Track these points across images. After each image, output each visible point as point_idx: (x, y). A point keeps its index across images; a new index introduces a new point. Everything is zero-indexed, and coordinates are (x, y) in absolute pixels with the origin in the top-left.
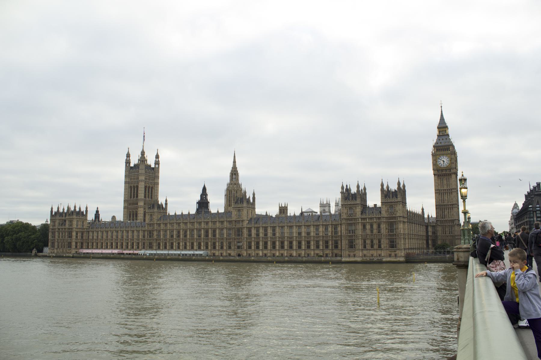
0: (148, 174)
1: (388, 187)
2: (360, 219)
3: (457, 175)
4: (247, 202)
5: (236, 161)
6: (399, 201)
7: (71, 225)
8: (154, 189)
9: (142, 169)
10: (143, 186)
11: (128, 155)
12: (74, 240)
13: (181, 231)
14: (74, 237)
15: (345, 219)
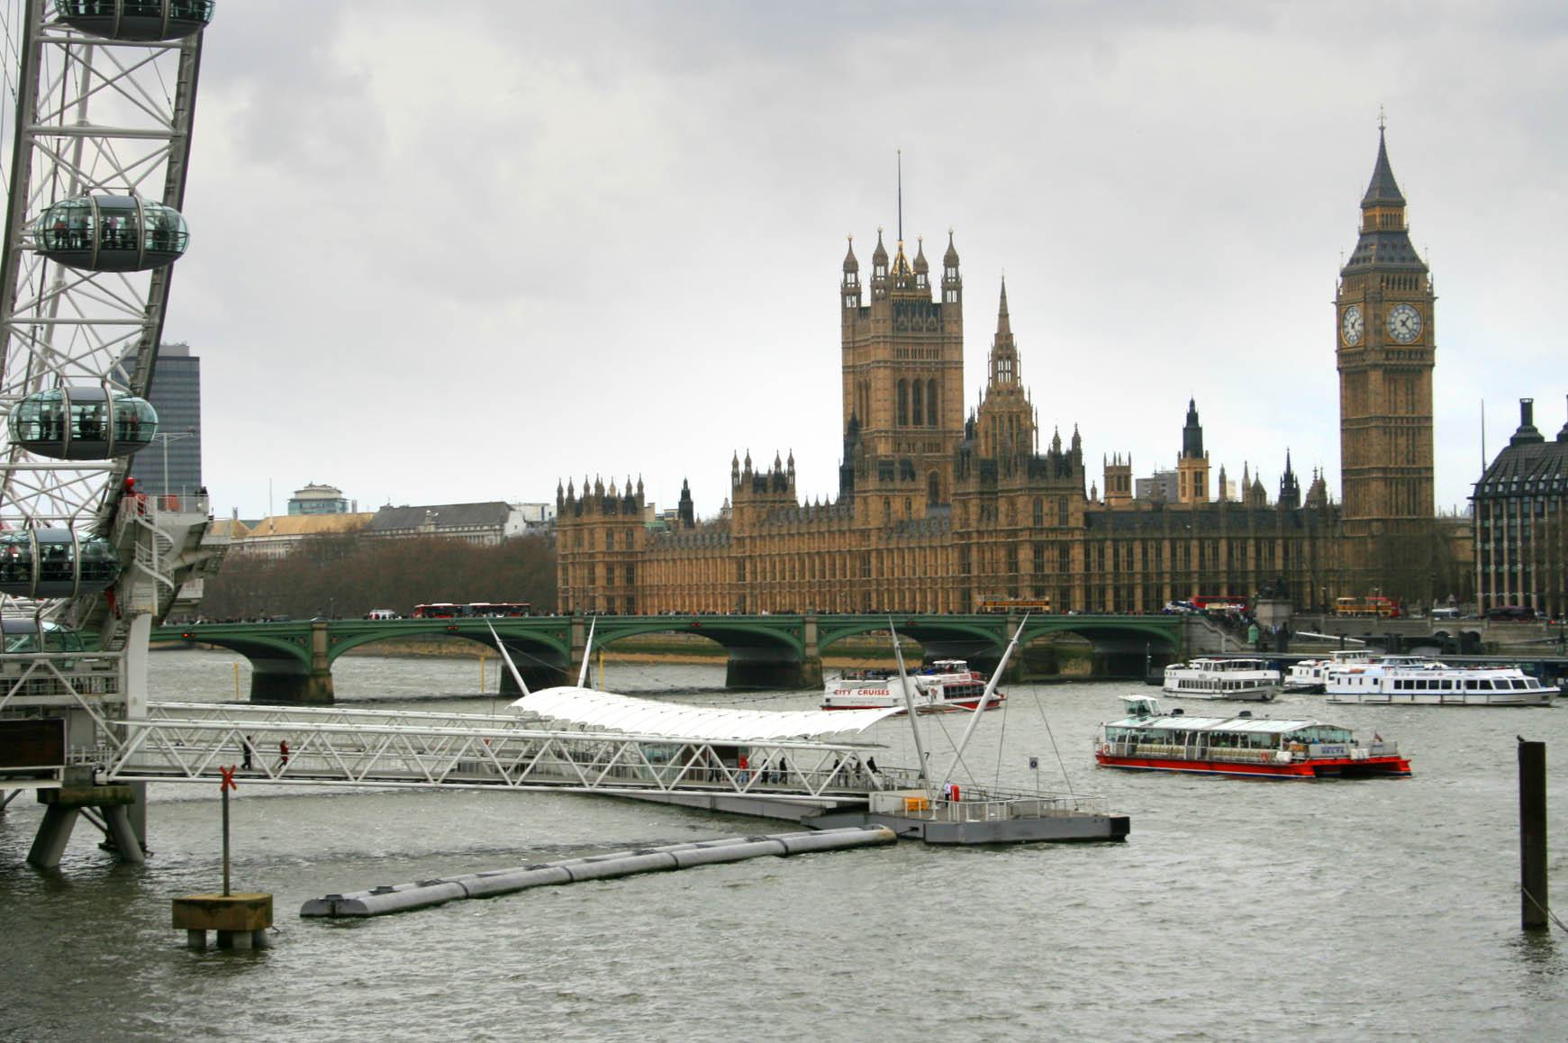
0: (910, 334)
1: (1057, 442)
2: (975, 535)
3: (1432, 366)
4: (882, 473)
5: (1009, 312)
6: (1019, 487)
7: (592, 545)
8: (943, 387)
9: (878, 321)
10: (888, 384)
11: (851, 266)
12: (600, 591)
13: (787, 558)
14: (601, 582)
15: (958, 533)
